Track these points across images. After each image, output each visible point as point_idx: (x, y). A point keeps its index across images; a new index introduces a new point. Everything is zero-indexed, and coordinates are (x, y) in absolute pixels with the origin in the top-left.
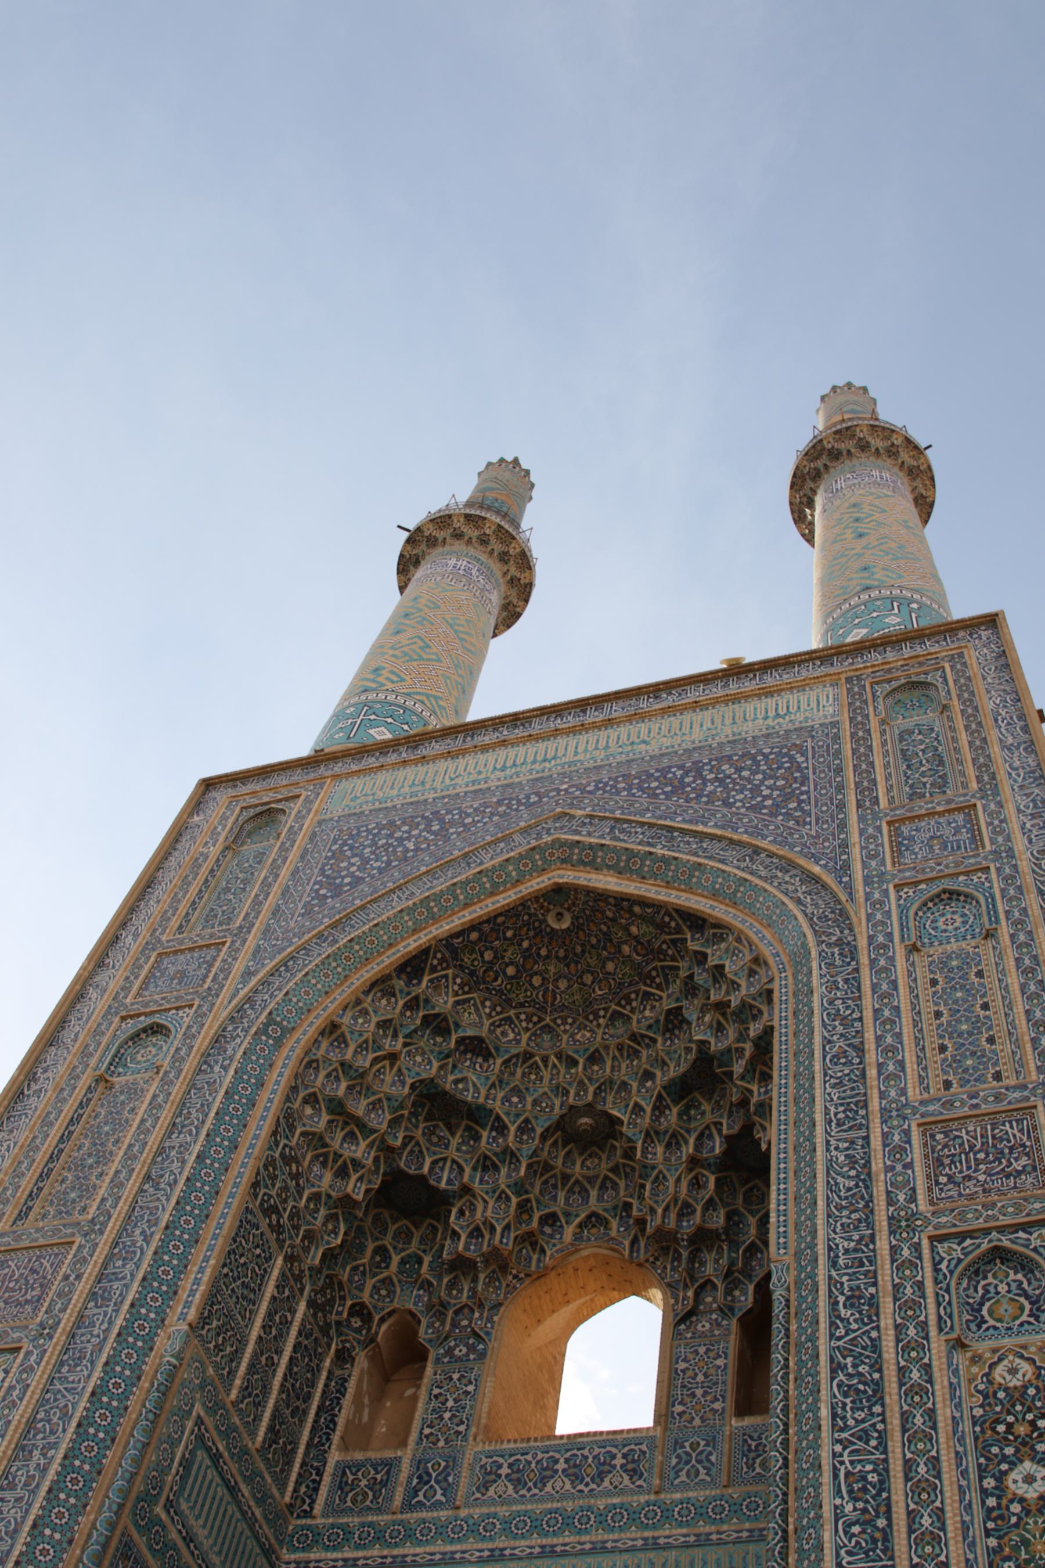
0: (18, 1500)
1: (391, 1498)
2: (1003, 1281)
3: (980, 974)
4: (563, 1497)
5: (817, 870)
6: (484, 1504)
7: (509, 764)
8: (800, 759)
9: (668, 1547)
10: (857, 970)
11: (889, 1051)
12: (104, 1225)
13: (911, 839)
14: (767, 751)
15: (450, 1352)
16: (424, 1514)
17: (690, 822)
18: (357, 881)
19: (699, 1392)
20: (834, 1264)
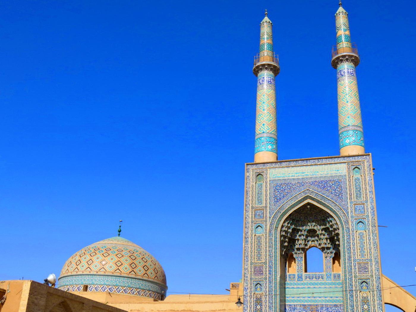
0: (271, 300)
1: (295, 279)
2: (364, 284)
3: (364, 237)
4: (315, 281)
5: (345, 212)
6: (307, 281)
7: (297, 173)
8: (341, 184)
9: (327, 288)
10: (350, 234)
11: (354, 250)
12: (267, 263)
13: (356, 209)
14: (336, 180)
15: (298, 259)
16: (300, 282)
17: (327, 196)
18: (280, 199)
19: (328, 268)
20: (349, 280)
